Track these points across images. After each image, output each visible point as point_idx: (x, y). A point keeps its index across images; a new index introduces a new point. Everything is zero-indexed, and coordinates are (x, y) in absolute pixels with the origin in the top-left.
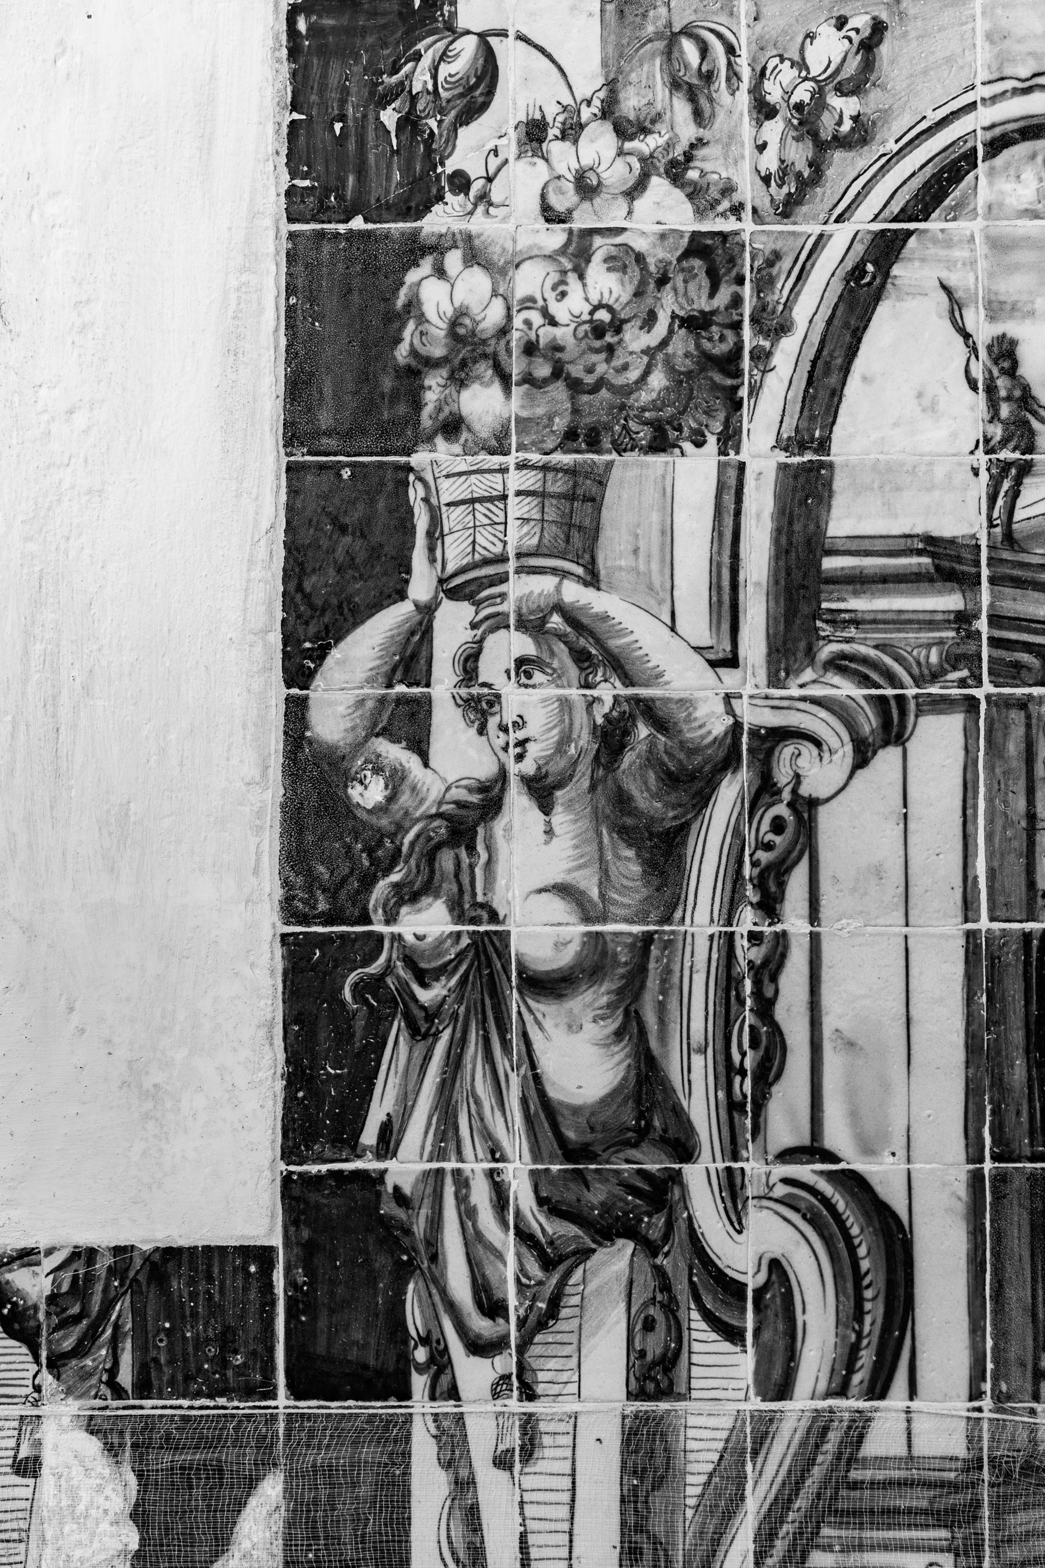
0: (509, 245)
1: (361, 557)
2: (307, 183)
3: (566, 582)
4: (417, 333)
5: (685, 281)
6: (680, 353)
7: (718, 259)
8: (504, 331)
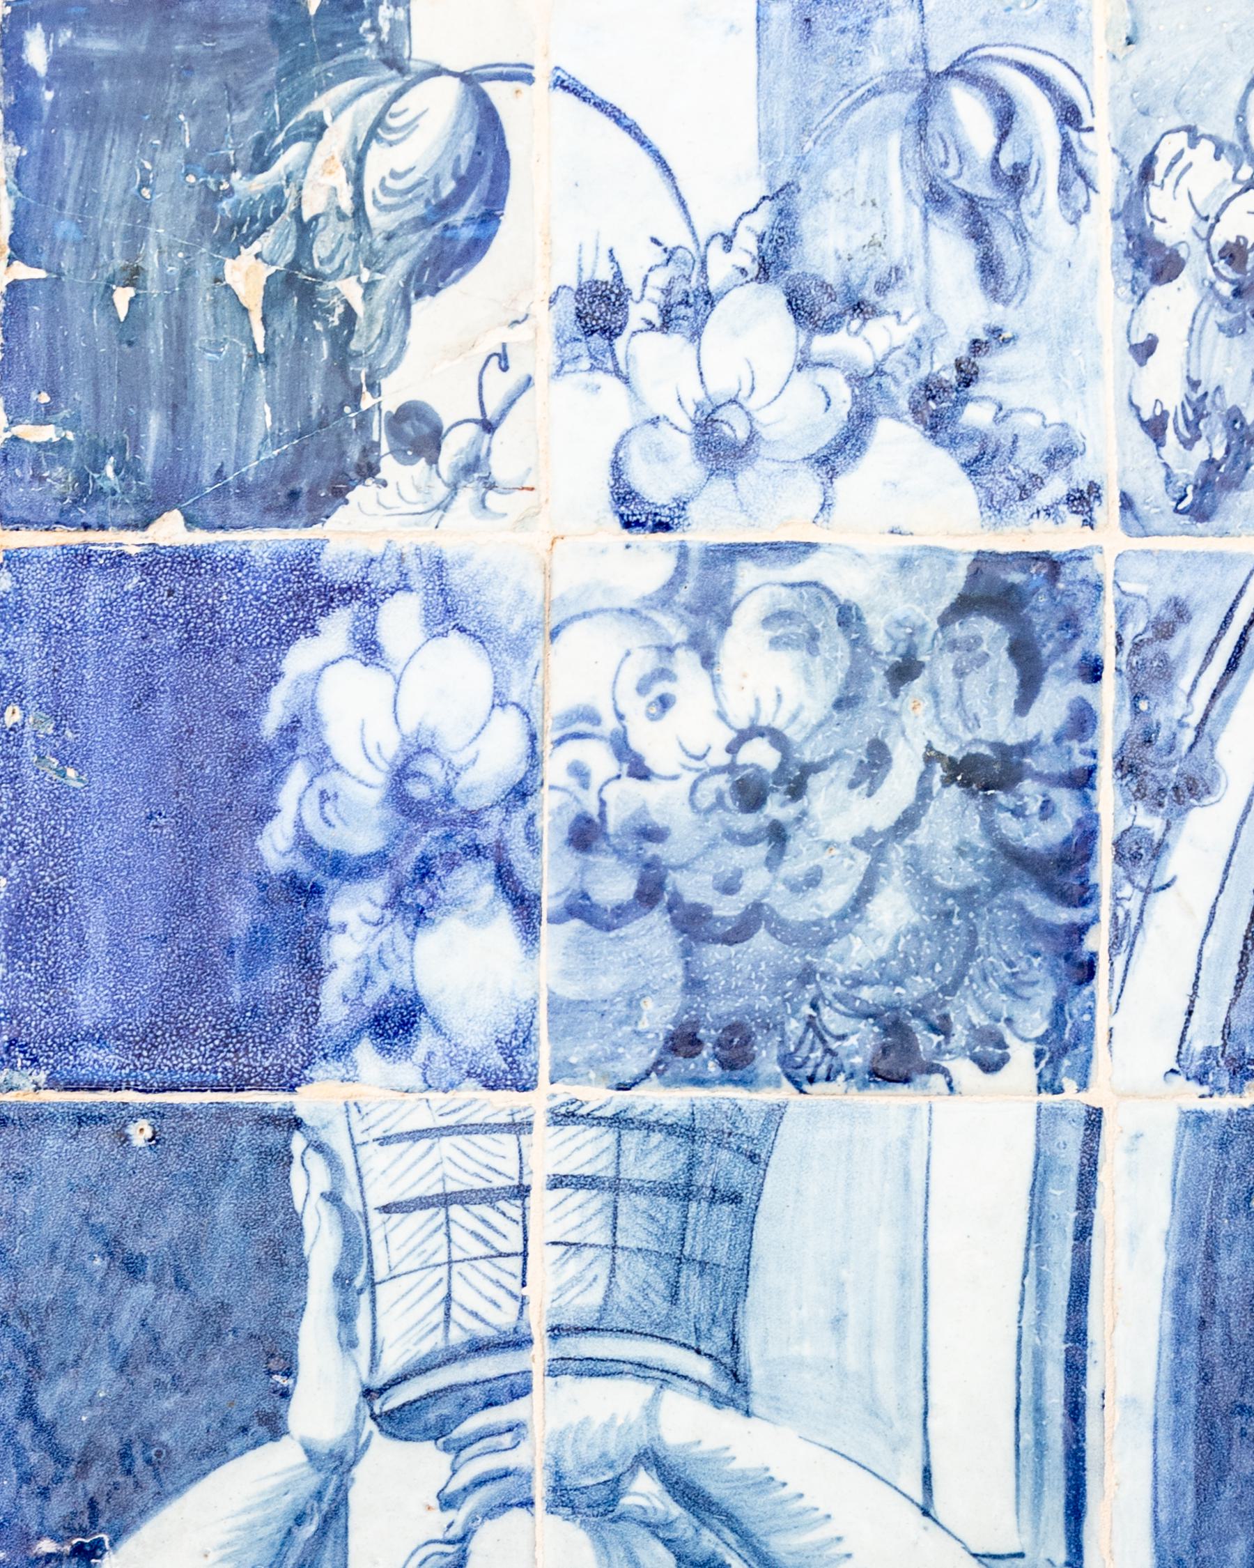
0: (534, 584)
1: (176, 1334)
2: (48, 433)
3: (668, 1395)
4: (313, 796)
5: (960, 673)
6: (947, 844)
7: (1038, 620)
8: (521, 792)
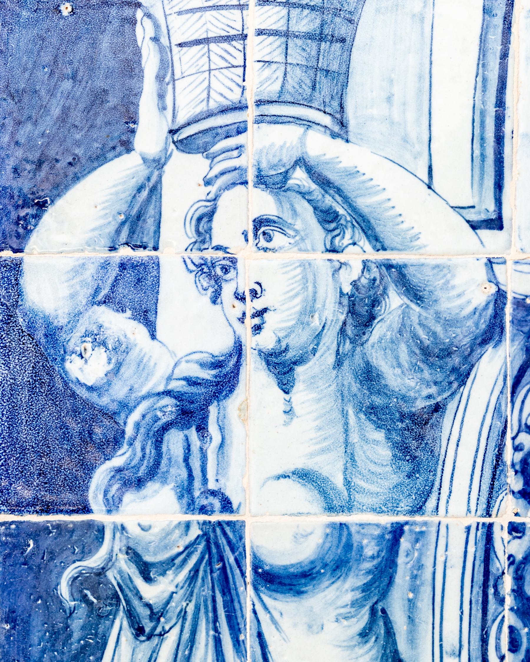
3: (310, 132)
